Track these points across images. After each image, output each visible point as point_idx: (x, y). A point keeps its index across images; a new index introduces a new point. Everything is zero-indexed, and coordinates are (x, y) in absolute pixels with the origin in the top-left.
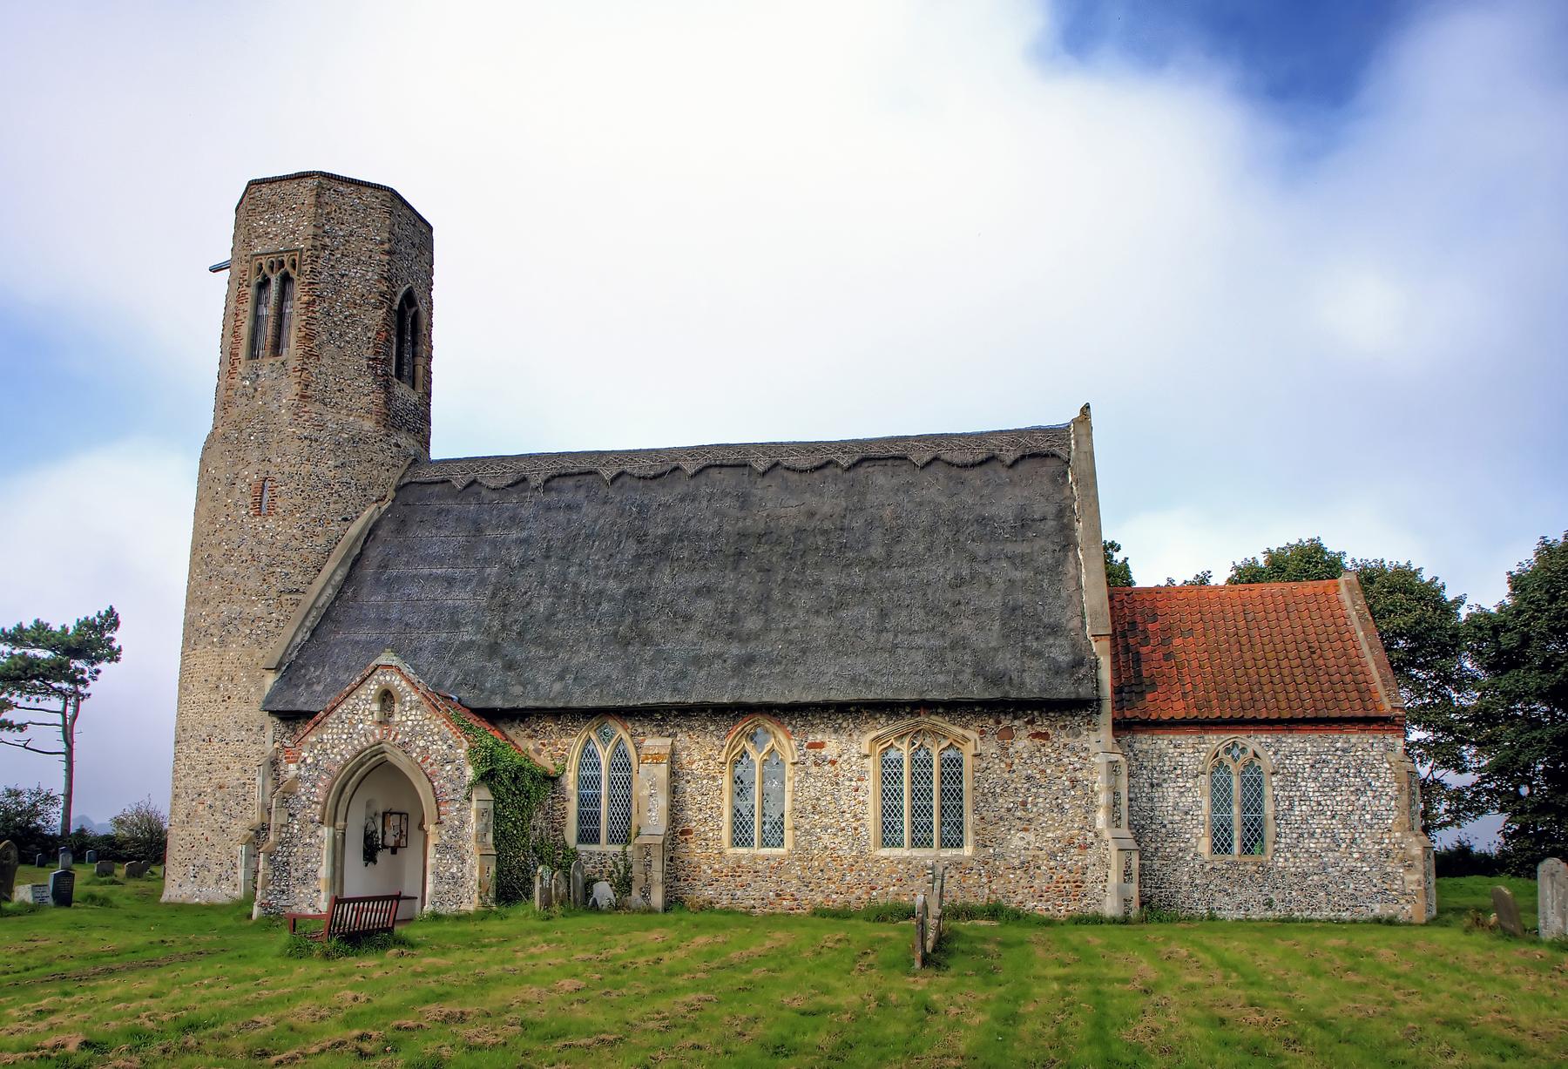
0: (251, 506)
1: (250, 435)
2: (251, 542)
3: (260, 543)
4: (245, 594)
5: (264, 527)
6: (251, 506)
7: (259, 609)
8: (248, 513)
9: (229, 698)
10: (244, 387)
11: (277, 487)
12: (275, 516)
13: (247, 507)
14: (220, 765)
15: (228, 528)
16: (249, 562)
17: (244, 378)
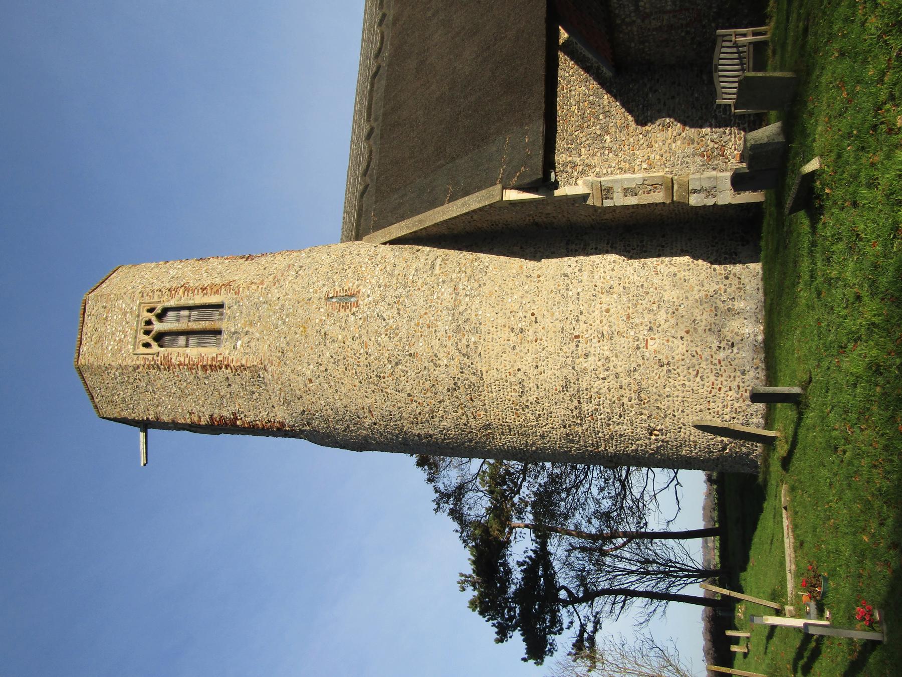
0: (348, 310)
1: (284, 323)
2: (381, 307)
3: (383, 298)
4: (430, 307)
5: (368, 296)
6: (348, 310)
7: (446, 292)
8: (354, 314)
9: (533, 314)
10: (242, 346)
11: (335, 289)
12: (361, 287)
13: (348, 316)
14: (604, 322)
15: (365, 338)
16: (400, 307)
17: (235, 347)
